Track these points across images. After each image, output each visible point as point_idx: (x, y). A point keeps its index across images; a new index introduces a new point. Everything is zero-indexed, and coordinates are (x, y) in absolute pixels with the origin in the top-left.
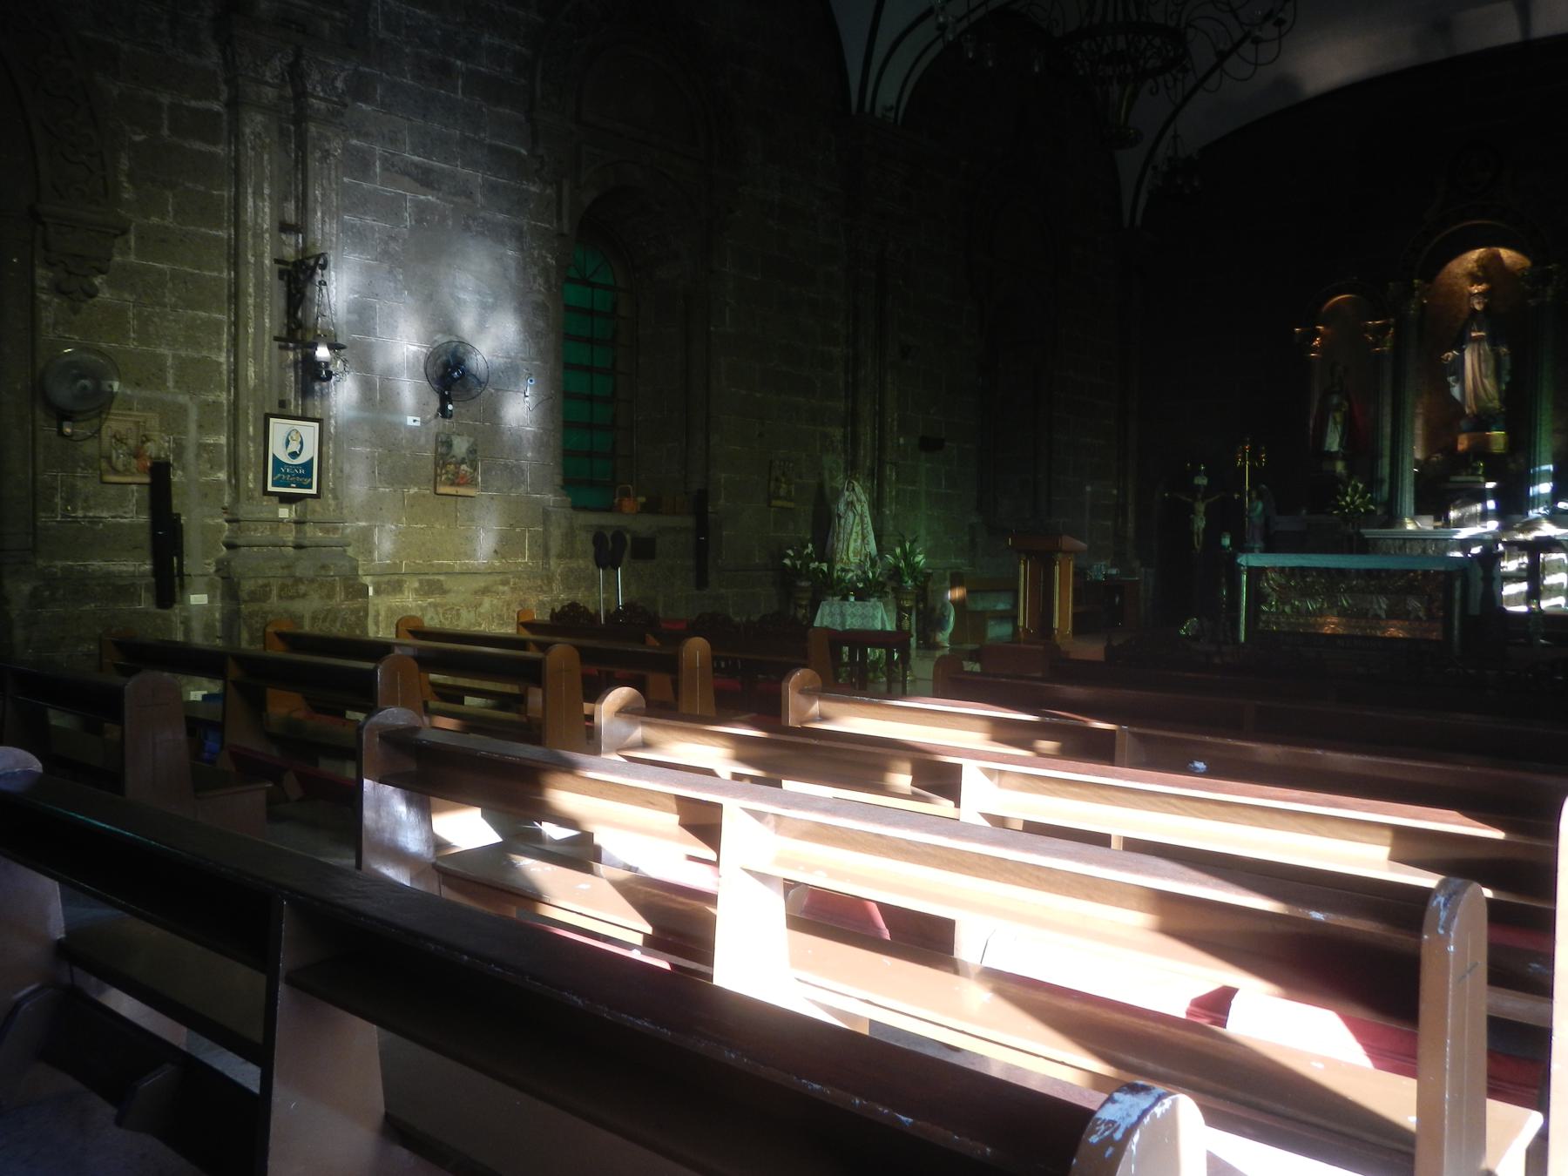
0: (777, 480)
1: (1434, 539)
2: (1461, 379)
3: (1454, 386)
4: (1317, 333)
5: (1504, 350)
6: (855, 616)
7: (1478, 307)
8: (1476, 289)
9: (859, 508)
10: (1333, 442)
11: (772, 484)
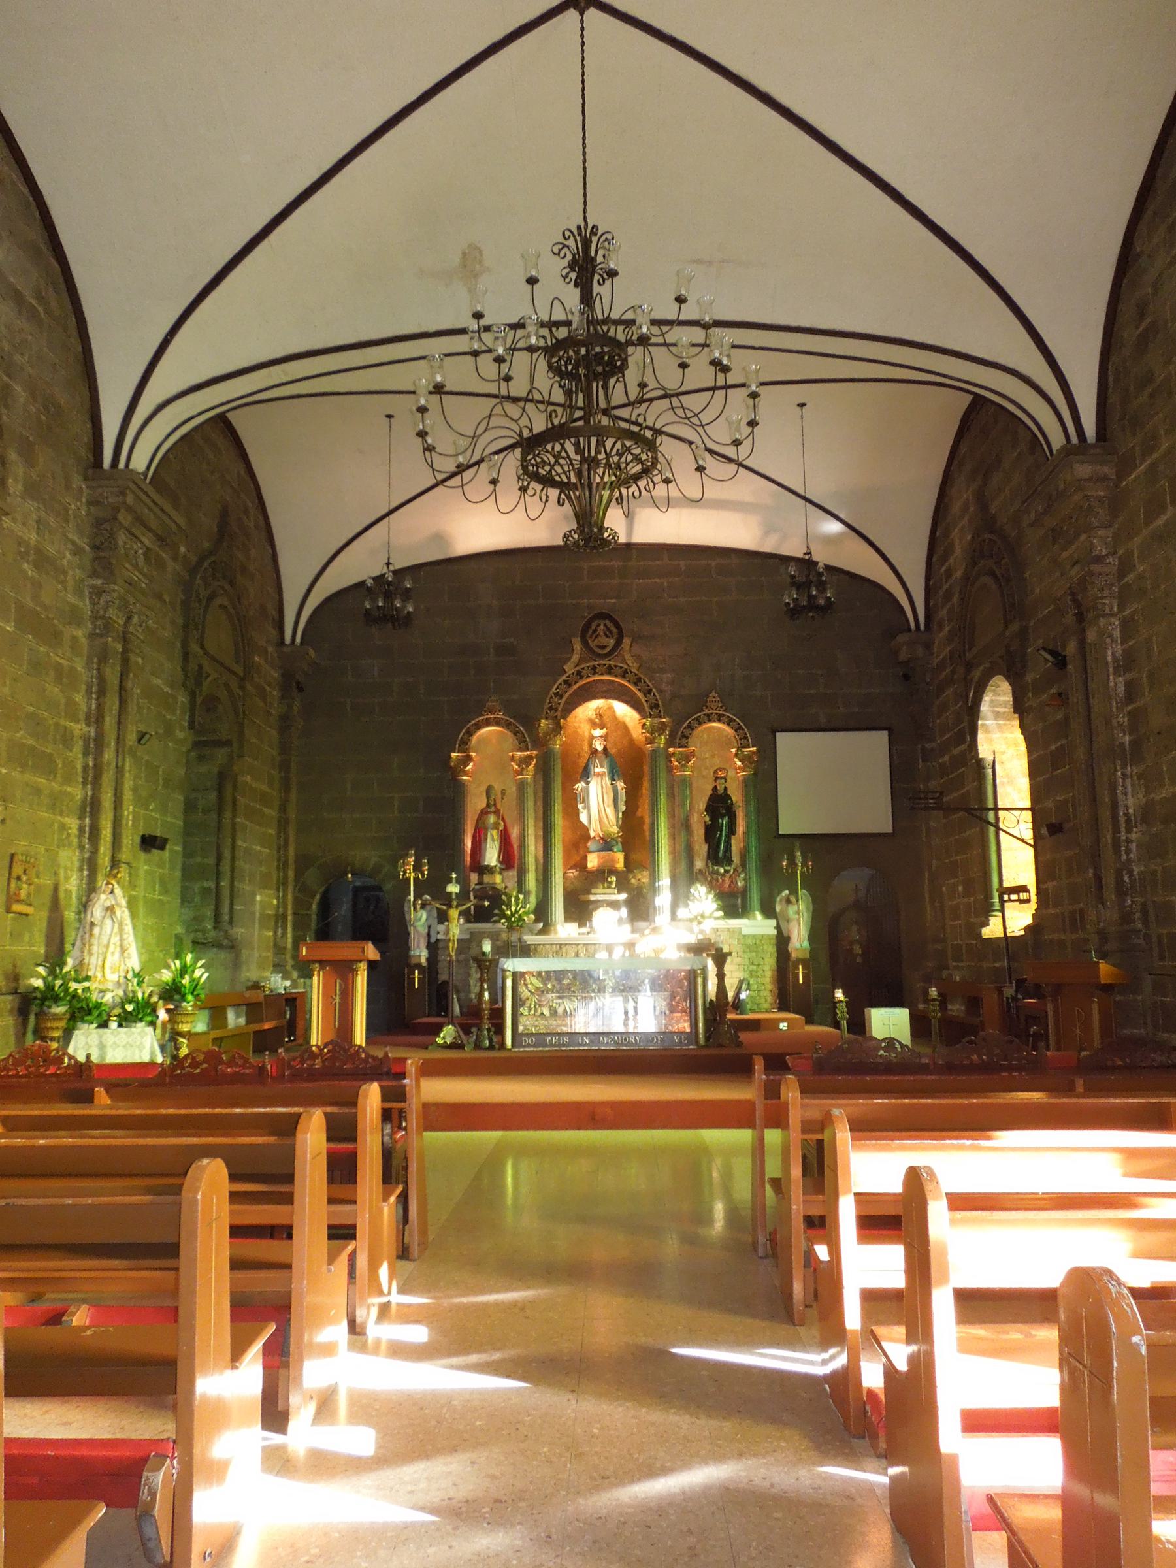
0: (19, 878)
1: (584, 944)
2: (587, 807)
4: (468, 759)
5: (620, 785)
6: (118, 1046)
7: (600, 748)
8: (598, 732)
9: (118, 913)
10: (492, 856)
11: (13, 885)
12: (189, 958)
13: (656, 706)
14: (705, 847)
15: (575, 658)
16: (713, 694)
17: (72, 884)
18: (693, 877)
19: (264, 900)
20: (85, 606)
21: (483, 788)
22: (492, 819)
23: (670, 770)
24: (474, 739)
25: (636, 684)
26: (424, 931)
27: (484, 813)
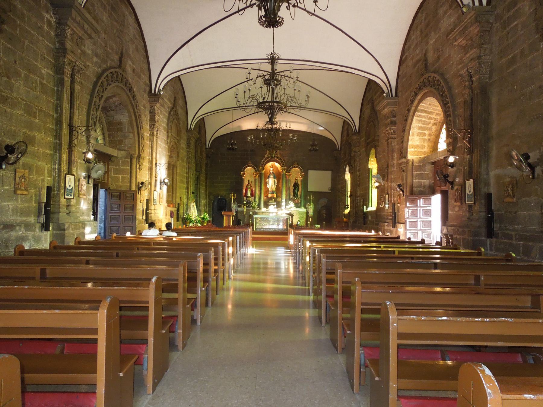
2: (269, 184)
4: (244, 174)
5: (276, 180)
7: (272, 172)
8: (272, 169)
10: (249, 194)
12: (206, 214)
13: (284, 165)
14: (293, 194)
15: (267, 154)
17: (185, 201)
18: (290, 199)
19: (203, 202)
20: (186, 154)
21: (247, 180)
22: (249, 186)
23: (286, 177)
24: (246, 170)
25: (280, 160)
26: (235, 209)
27: (247, 185)
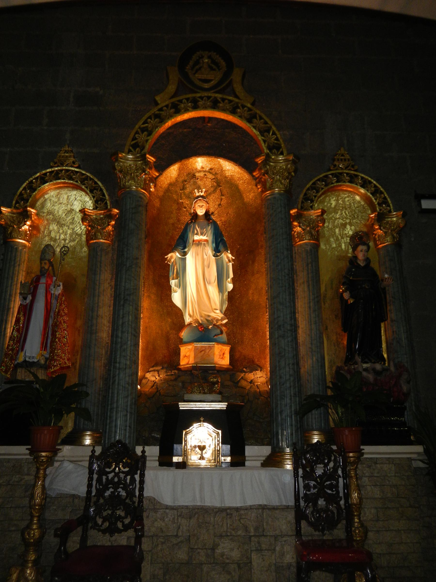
3: (176, 292)
7: (201, 212)
15: (172, 88)
16: (342, 151)
25: (249, 121)
